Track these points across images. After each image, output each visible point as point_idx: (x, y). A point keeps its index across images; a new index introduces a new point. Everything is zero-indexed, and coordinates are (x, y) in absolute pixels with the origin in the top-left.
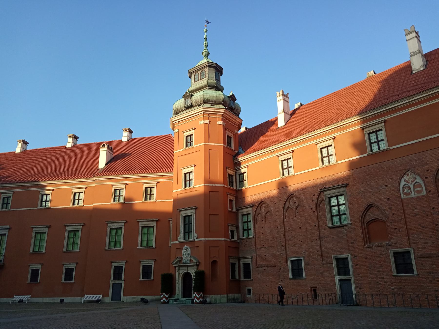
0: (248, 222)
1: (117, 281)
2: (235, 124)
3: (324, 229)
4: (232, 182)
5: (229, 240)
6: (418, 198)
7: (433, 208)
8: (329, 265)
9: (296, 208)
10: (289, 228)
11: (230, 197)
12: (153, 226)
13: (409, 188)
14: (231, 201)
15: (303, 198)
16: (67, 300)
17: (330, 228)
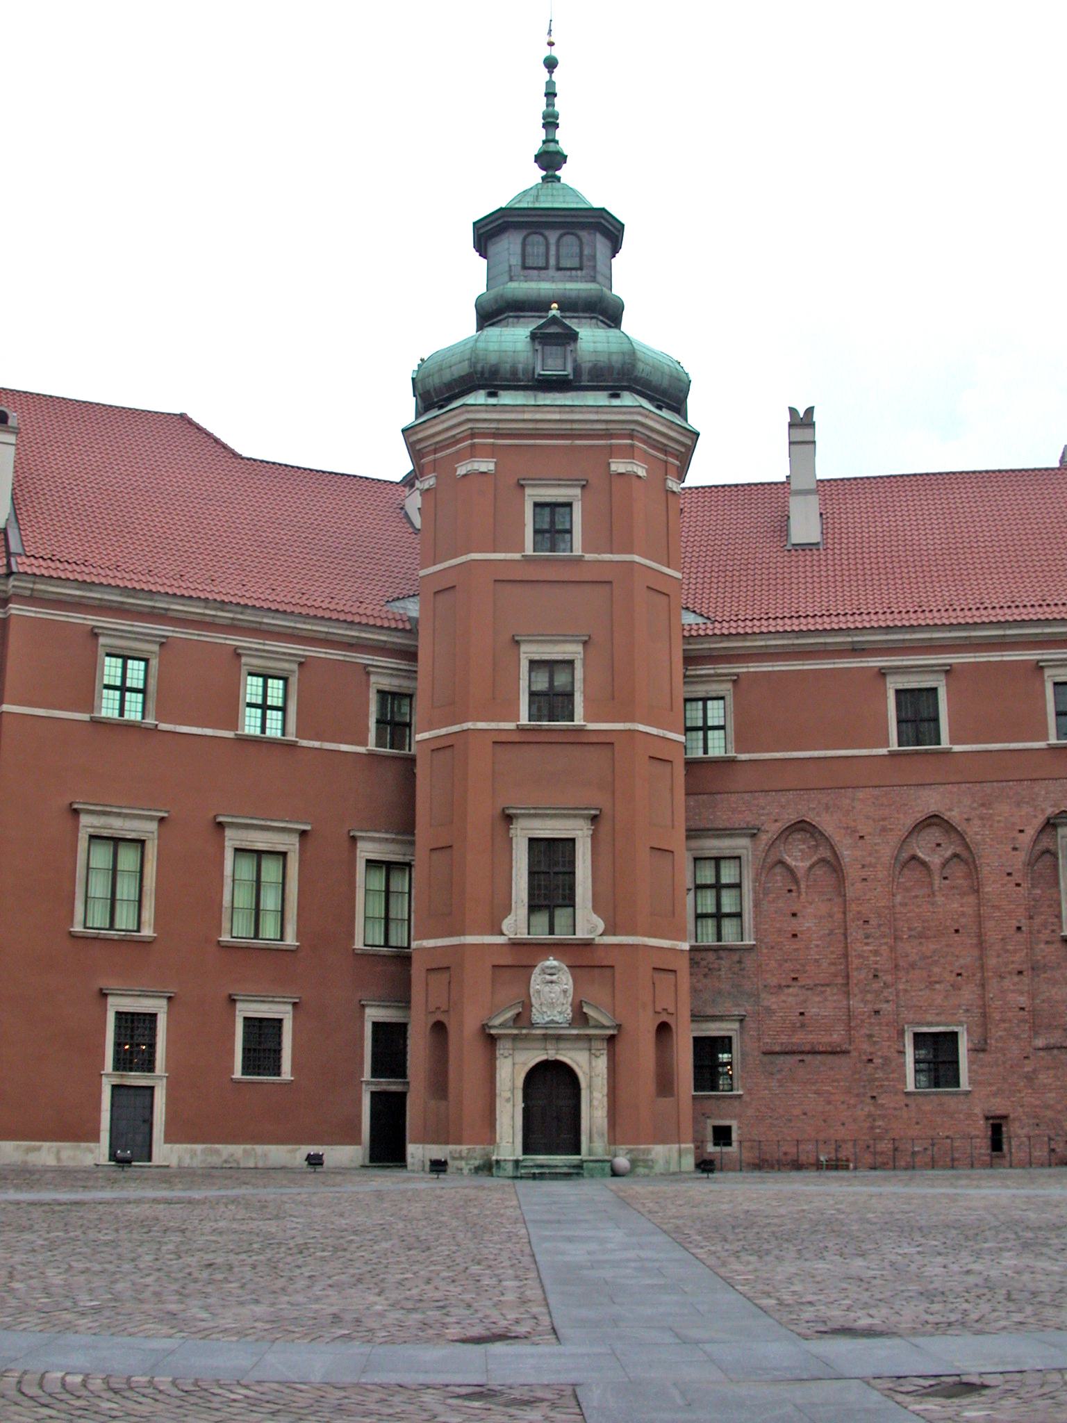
1: (136, 1079)
3: (1047, 943)
8: (1055, 1052)
9: (944, 865)
10: (910, 929)
12: (284, 855)
15: (977, 833)
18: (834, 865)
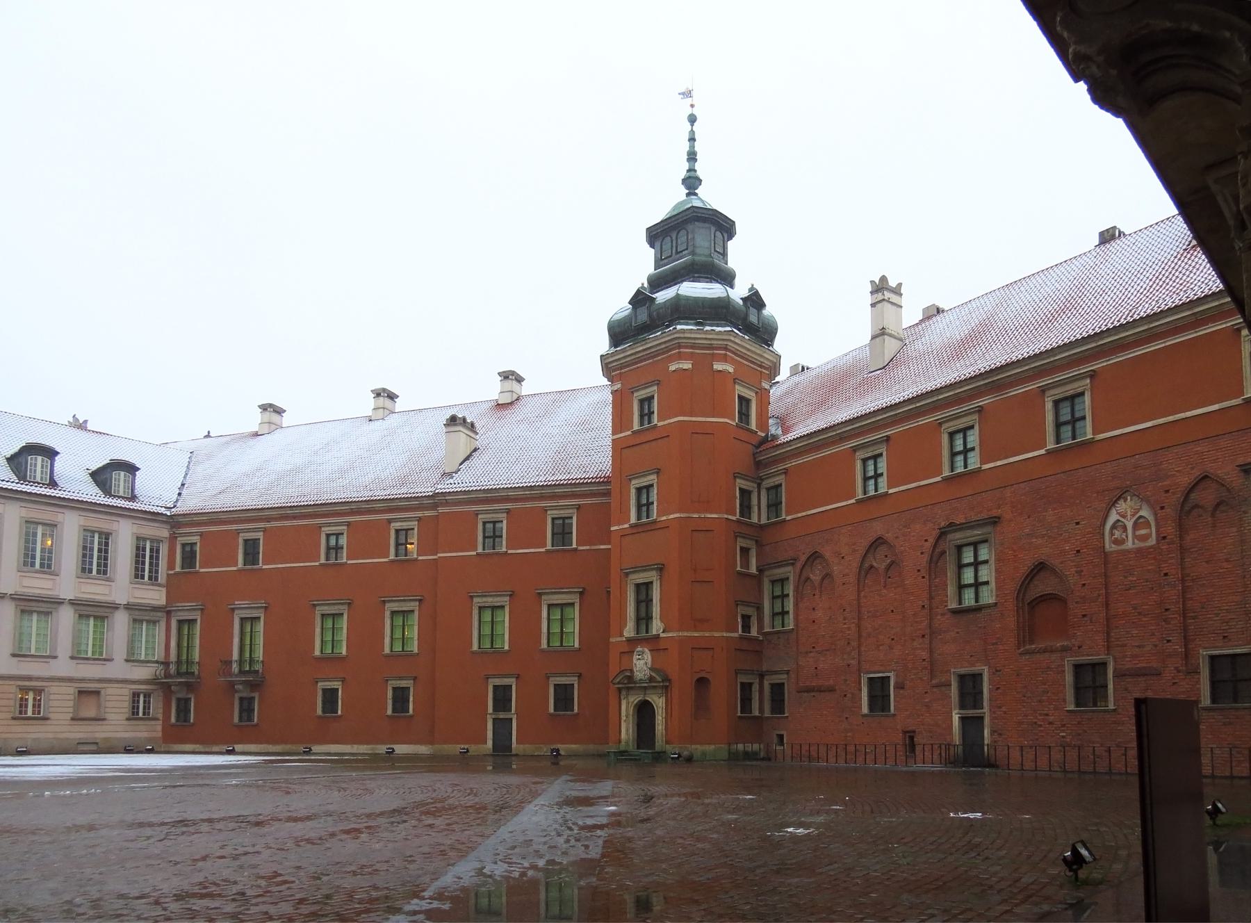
0: (784, 596)
2: (760, 366)
4: (749, 507)
5: (735, 635)
6: (1139, 550)
7: (1166, 574)
11: (741, 542)
13: (1125, 528)
14: (745, 551)
16: (401, 749)
17: (955, 612)
18: (827, 576)
